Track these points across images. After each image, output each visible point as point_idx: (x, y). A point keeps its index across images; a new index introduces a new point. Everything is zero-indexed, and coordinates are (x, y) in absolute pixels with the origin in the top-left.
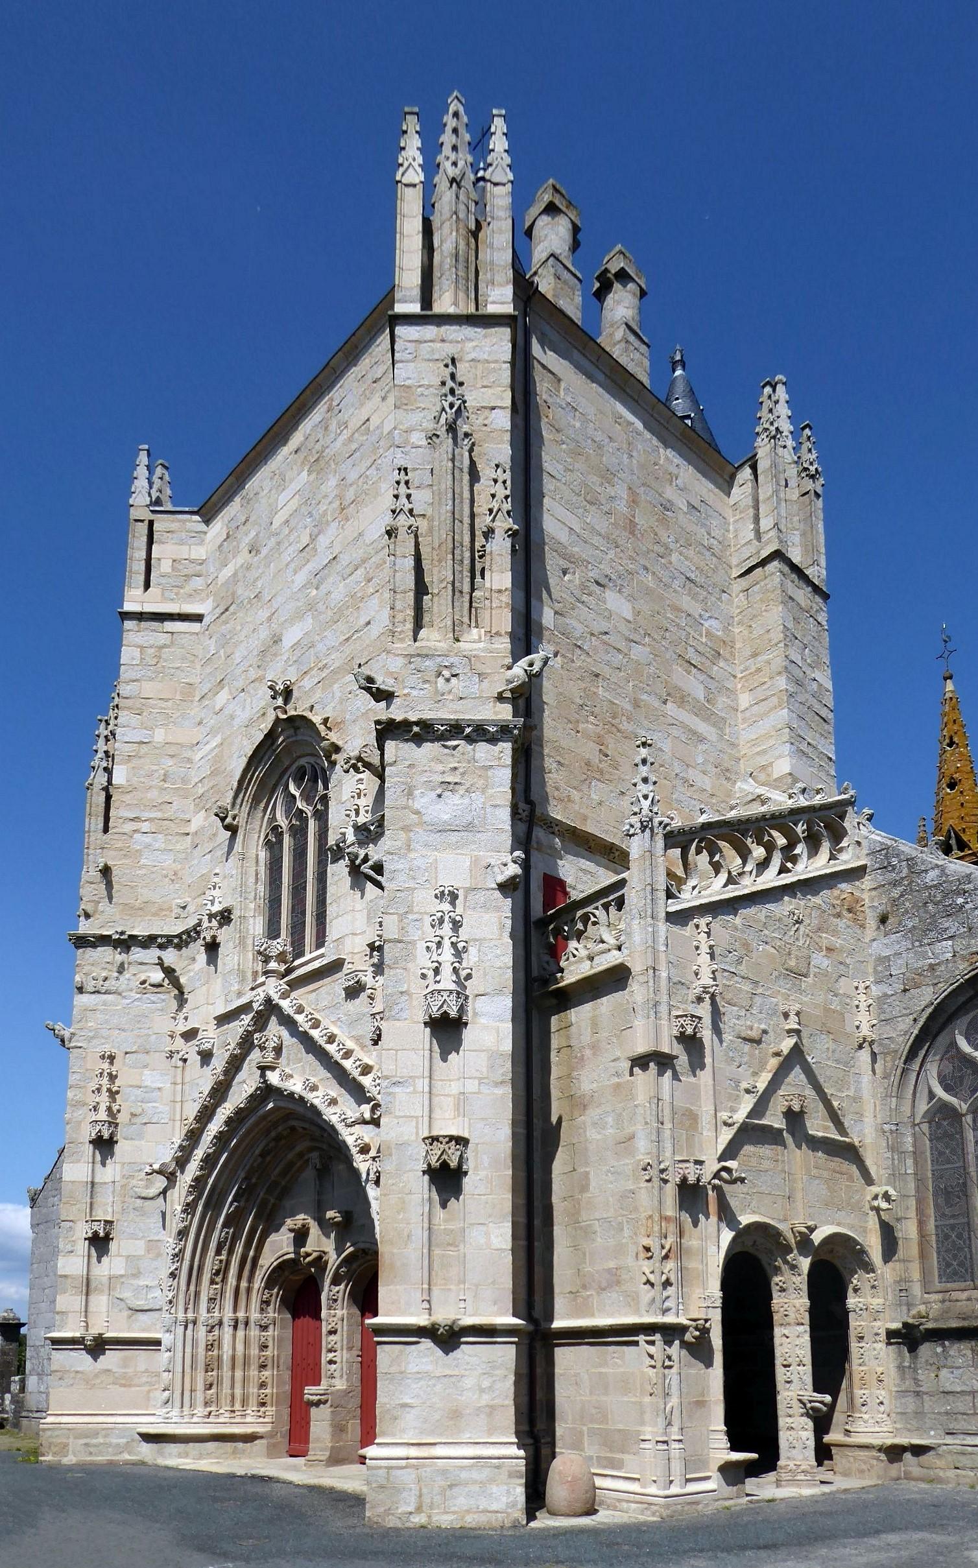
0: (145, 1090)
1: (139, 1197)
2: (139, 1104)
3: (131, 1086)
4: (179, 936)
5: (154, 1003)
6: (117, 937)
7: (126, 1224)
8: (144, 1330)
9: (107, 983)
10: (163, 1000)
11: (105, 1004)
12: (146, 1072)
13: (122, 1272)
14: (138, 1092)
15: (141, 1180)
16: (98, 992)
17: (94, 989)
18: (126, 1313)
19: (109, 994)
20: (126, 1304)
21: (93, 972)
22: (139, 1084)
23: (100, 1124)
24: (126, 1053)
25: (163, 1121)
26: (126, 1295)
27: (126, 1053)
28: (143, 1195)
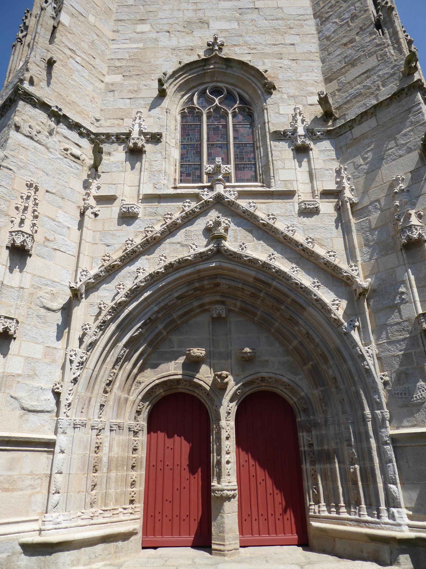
1: (44, 307)
2: (52, 232)
3: (48, 217)
4: (97, 135)
5: (71, 167)
6: (56, 110)
7: (28, 327)
8: (33, 431)
9: (39, 135)
10: (78, 169)
11: (35, 148)
12: (60, 211)
13: (20, 372)
14: (53, 223)
15: (46, 293)
16: (32, 138)
17: (29, 134)
19: (40, 144)
21: (30, 122)
22: (53, 217)
23: (26, 236)
24: (47, 191)
25: (68, 252)
26: (21, 394)
27: (47, 191)
28: (48, 306)
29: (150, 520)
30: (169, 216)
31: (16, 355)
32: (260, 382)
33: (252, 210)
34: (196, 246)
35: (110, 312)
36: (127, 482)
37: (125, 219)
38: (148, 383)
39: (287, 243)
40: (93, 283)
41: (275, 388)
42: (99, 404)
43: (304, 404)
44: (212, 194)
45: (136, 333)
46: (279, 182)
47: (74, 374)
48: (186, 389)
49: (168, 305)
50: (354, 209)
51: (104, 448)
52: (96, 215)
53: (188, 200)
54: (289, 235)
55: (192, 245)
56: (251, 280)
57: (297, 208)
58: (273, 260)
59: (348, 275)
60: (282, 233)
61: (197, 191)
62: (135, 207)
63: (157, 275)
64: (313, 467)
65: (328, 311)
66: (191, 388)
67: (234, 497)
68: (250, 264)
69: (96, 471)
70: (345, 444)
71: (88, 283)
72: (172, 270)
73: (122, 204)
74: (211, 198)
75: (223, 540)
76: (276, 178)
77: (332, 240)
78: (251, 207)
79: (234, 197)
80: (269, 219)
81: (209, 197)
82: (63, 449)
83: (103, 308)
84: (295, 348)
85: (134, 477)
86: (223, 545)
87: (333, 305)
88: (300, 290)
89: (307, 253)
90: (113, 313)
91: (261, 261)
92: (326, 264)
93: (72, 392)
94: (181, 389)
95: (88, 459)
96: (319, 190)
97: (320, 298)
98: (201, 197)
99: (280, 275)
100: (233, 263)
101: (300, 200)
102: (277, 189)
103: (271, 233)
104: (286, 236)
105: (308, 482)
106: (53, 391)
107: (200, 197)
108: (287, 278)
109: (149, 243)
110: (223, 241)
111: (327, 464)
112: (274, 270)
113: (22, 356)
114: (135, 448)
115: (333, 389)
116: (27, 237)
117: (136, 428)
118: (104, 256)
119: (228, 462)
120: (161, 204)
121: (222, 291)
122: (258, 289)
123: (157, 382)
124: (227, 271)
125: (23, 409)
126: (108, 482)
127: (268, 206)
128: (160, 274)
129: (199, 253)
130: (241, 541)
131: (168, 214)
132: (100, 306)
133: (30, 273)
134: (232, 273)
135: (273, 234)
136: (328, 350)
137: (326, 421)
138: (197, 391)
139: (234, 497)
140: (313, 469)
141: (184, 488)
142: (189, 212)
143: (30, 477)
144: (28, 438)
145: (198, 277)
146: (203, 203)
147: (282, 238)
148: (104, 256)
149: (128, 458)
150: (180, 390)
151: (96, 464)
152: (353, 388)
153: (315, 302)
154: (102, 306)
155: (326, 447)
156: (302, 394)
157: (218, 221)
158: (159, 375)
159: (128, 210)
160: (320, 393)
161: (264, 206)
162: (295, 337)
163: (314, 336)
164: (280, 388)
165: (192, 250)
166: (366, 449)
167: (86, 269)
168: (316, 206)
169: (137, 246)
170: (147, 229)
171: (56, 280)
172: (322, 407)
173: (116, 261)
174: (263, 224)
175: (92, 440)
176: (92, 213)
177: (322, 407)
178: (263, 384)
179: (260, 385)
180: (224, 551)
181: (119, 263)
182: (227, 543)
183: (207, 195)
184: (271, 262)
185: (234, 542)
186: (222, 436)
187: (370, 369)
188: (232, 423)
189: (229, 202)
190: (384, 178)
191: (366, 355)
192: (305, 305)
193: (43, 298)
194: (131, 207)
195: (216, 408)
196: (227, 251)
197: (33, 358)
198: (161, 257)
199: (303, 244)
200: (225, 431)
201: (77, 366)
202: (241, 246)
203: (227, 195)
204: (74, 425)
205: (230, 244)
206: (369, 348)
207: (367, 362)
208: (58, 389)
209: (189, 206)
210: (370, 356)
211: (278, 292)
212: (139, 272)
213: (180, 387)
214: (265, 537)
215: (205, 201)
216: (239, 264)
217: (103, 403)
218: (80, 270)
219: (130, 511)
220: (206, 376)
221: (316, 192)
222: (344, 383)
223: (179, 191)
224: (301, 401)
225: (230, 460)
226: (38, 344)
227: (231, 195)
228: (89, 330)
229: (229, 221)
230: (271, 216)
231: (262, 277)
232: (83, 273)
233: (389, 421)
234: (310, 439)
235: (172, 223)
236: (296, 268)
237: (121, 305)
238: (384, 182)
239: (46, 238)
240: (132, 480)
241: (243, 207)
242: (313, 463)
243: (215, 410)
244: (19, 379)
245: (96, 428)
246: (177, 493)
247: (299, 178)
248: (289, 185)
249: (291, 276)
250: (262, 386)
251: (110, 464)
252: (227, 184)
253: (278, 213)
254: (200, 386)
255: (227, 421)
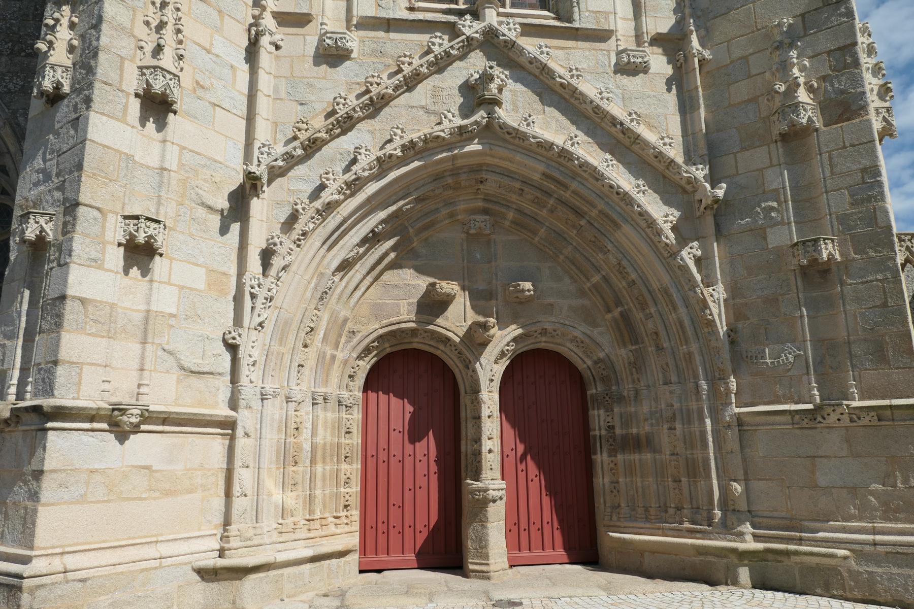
0: (214, 59)
1: (203, 204)
13: (173, 311)
15: (204, 180)
18: (175, 374)
20: (177, 359)
23: (168, 76)
25: (235, 111)
28: (209, 203)
29: (370, 533)
30: (407, 59)
31: (165, 283)
32: (539, 336)
33: (543, 58)
34: (453, 114)
35: (314, 218)
36: (339, 480)
37: (330, 59)
38: (367, 334)
39: (596, 119)
40: (280, 167)
41: (559, 344)
42: (297, 364)
43: (604, 369)
44: (478, 26)
45: (352, 254)
46: (587, 14)
47: (259, 315)
48: (425, 344)
49: (402, 210)
50: (705, 70)
51: (305, 430)
52: (278, 47)
53: (438, 34)
54: (602, 106)
55: (446, 112)
56: (536, 177)
57: (613, 60)
58: (576, 145)
59: (691, 177)
60: (592, 102)
61: (452, 18)
62: (348, 38)
63: (389, 160)
64: (613, 458)
65: (657, 233)
66: (432, 343)
67: (501, 498)
68: (539, 150)
69: (296, 463)
70: (665, 427)
71: (273, 167)
72: (412, 152)
73: (323, 31)
74: (477, 32)
75: (487, 557)
76: (582, 6)
77: (666, 119)
78: (542, 53)
79: (515, 34)
80: (572, 76)
81: (474, 30)
82: (248, 431)
83: (301, 211)
84: (595, 286)
85: (348, 474)
86: (487, 564)
87: (665, 222)
88: (615, 197)
89: (629, 138)
90: (318, 219)
91: (557, 147)
92: (656, 157)
93: (256, 344)
94: (417, 344)
95: (283, 445)
96: (651, 33)
97: (646, 211)
98: (460, 29)
99: (586, 171)
100: (510, 147)
101: (620, 48)
102: (583, 26)
103: (572, 100)
104: (598, 107)
105: (603, 478)
106: (225, 341)
107: (457, 30)
108: (597, 176)
109: (372, 105)
110: (497, 108)
111: (634, 453)
112: (576, 162)
113: (174, 285)
114: (348, 430)
115: (651, 349)
116: (171, 80)
117: (349, 402)
118: (298, 122)
119: (490, 451)
120: (392, 35)
121: (486, 191)
122: (546, 192)
123: (381, 332)
124: (500, 159)
125: (183, 368)
126: (313, 479)
127: (567, 54)
128: (394, 158)
129: (457, 127)
130: (509, 559)
131: (405, 56)
132: (295, 207)
133: (178, 145)
134: (507, 163)
135: (576, 103)
136: (649, 291)
137: (637, 392)
138: (442, 347)
139: (501, 498)
140: (612, 461)
141: (420, 488)
142: (440, 54)
143: (199, 473)
144: (195, 414)
145: (451, 167)
146: (463, 41)
147: (591, 111)
148: (298, 122)
149: (339, 445)
150: (415, 346)
151: (295, 453)
152: (685, 347)
153: (636, 217)
154: (299, 207)
155: (635, 431)
156: (602, 355)
157: (491, 74)
158: (384, 322)
159: (336, 42)
160: (631, 355)
161: (560, 53)
162: (597, 270)
163: (629, 269)
164: (569, 345)
165: (447, 120)
166: (697, 433)
167: (268, 143)
168: (646, 60)
169: (354, 108)
170: (370, 79)
171: (218, 158)
172: (632, 374)
173: (320, 132)
174: (562, 85)
175: (289, 418)
176: (271, 43)
177: (632, 374)
178: (544, 339)
179: (538, 340)
180: (488, 572)
181: (324, 135)
182: (491, 561)
183: (470, 27)
184: (572, 149)
185: (500, 560)
186: (483, 415)
187: (714, 321)
188: (496, 396)
189: (505, 41)
190: (758, 20)
191: (709, 300)
192: (619, 221)
193: (201, 189)
194: (341, 38)
195: (472, 374)
196: (503, 127)
197: (191, 289)
198: (395, 130)
199: (624, 122)
200: (487, 406)
201: (263, 304)
202: (526, 120)
203: (503, 29)
204: (262, 394)
205: (506, 114)
206: (714, 290)
207: (710, 310)
208: (234, 338)
209: (440, 45)
210: (714, 302)
211: (578, 199)
212: (360, 154)
213: (416, 340)
214: (538, 553)
215: (468, 38)
216: (520, 150)
217: (302, 363)
218: (257, 144)
219: (346, 521)
220: (458, 325)
221: (645, 35)
222: (670, 340)
223: (420, 16)
224: (599, 365)
225: (492, 448)
226: (198, 265)
227: (510, 29)
228: (279, 246)
229: (506, 76)
230: (574, 72)
231: (557, 175)
232: (262, 149)
233: (735, 394)
234: (609, 419)
235: (412, 72)
236: (611, 161)
237: (330, 207)
238: (759, 28)
239: (197, 83)
240: (346, 477)
241: (529, 53)
242: (613, 453)
243: (471, 376)
244: (172, 321)
245: (294, 399)
246: (409, 495)
247: (619, 9)
248: (603, 20)
249: (603, 174)
250: (540, 342)
251: (314, 454)
252: (501, 10)
253: (584, 67)
254: (448, 339)
255: (490, 392)
